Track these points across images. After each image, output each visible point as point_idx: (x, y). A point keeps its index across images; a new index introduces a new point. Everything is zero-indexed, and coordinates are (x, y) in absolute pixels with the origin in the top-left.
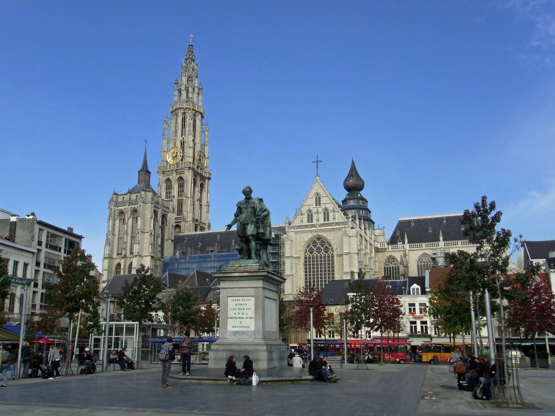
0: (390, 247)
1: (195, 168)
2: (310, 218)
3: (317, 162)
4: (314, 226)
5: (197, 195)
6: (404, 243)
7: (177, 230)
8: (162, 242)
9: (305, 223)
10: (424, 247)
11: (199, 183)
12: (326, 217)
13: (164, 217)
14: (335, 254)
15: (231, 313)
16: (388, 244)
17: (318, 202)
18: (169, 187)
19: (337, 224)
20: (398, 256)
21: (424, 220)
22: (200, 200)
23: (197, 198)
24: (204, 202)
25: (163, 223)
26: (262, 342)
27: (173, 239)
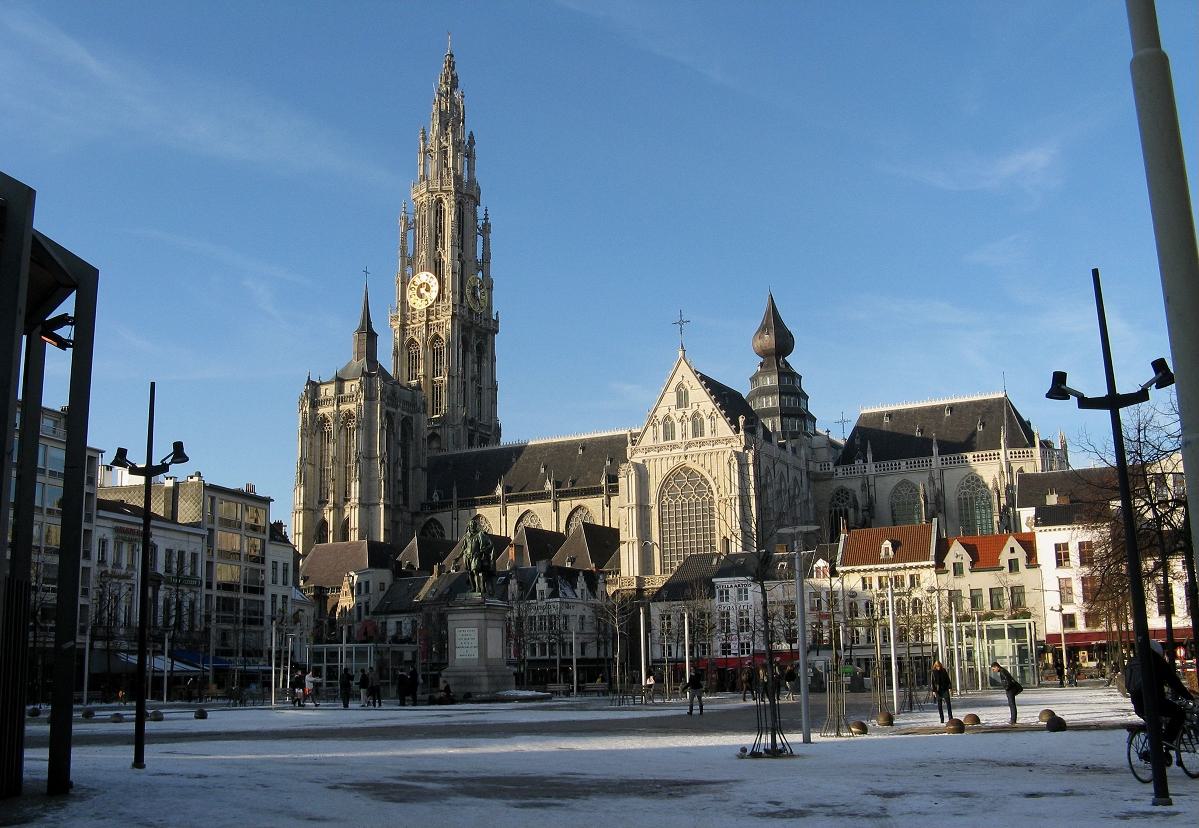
0: (840, 470)
1: (466, 313)
2: (669, 434)
3: (681, 323)
4: (674, 447)
5: (472, 368)
6: (865, 461)
7: (435, 445)
8: (405, 474)
9: (661, 441)
10: (903, 468)
11: (474, 342)
12: (698, 430)
13: (406, 423)
14: (716, 496)
15: (458, 644)
16: (837, 464)
17: (682, 399)
18: (413, 361)
19: (718, 441)
20: (854, 485)
21: (908, 412)
22: (477, 379)
23: (469, 374)
24: (485, 380)
25: (404, 434)
26: (483, 668)
27: (425, 465)
